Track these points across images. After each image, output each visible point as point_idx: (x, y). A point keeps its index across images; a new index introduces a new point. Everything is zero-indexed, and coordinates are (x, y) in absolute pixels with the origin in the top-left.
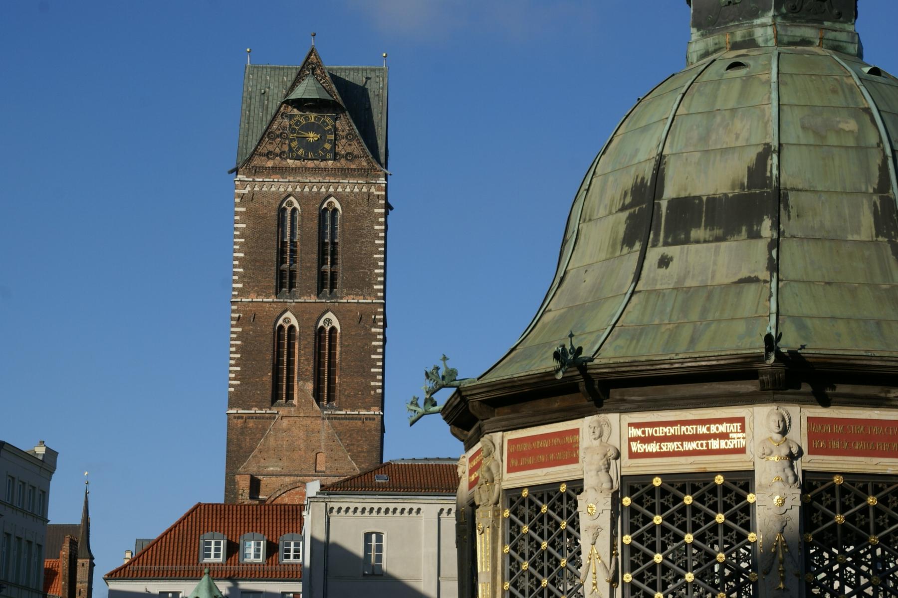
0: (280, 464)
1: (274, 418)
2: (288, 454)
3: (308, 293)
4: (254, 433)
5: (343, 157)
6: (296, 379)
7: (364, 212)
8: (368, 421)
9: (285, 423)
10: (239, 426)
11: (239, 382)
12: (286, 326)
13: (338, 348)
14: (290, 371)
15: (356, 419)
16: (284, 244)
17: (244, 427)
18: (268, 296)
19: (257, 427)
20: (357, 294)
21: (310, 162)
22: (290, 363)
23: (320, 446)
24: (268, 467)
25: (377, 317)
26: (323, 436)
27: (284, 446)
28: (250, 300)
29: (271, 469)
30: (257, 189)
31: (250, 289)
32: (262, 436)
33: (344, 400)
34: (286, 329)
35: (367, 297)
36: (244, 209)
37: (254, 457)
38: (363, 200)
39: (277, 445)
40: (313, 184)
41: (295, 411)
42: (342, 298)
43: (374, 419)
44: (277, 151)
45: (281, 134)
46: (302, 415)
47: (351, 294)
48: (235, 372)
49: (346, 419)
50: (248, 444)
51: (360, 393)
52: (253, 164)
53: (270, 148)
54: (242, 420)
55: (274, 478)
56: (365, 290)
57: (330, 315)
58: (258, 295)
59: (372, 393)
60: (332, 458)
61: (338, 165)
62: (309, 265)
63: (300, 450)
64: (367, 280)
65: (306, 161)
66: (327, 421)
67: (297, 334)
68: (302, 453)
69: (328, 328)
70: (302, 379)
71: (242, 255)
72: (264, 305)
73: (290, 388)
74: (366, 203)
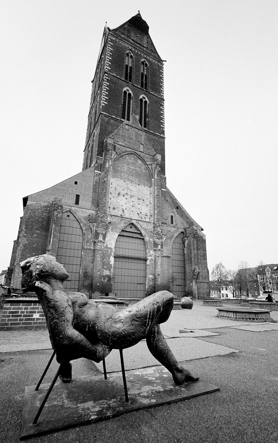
0: (125, 143)
6: (131, 113)
8: (160, 139)
9: (127, 127)
11: (107, 103)
12: (128, 92)
13: (147, 109)
14: (129, 110)
15: (156, 136)
17: (108, 122)
19: (114, 124)
22: (129, 107)
24: (119, 142)
26: (143, 137)
29: (120, 143)
32: (117, 129)
39: (123, 135)
41: (131, 124)
44: (126, 34)
46: (134, 126)
49: (152, 135)
50: (110, 129)
54: (108, 119)
58: (117, 75)
59: (162, 129)
66: (144, 133)
67: (132, 97)
68: (134, 141)
69: (144, 100)
72: (119, 80)
73: (128, 116)
74: (157, 67)
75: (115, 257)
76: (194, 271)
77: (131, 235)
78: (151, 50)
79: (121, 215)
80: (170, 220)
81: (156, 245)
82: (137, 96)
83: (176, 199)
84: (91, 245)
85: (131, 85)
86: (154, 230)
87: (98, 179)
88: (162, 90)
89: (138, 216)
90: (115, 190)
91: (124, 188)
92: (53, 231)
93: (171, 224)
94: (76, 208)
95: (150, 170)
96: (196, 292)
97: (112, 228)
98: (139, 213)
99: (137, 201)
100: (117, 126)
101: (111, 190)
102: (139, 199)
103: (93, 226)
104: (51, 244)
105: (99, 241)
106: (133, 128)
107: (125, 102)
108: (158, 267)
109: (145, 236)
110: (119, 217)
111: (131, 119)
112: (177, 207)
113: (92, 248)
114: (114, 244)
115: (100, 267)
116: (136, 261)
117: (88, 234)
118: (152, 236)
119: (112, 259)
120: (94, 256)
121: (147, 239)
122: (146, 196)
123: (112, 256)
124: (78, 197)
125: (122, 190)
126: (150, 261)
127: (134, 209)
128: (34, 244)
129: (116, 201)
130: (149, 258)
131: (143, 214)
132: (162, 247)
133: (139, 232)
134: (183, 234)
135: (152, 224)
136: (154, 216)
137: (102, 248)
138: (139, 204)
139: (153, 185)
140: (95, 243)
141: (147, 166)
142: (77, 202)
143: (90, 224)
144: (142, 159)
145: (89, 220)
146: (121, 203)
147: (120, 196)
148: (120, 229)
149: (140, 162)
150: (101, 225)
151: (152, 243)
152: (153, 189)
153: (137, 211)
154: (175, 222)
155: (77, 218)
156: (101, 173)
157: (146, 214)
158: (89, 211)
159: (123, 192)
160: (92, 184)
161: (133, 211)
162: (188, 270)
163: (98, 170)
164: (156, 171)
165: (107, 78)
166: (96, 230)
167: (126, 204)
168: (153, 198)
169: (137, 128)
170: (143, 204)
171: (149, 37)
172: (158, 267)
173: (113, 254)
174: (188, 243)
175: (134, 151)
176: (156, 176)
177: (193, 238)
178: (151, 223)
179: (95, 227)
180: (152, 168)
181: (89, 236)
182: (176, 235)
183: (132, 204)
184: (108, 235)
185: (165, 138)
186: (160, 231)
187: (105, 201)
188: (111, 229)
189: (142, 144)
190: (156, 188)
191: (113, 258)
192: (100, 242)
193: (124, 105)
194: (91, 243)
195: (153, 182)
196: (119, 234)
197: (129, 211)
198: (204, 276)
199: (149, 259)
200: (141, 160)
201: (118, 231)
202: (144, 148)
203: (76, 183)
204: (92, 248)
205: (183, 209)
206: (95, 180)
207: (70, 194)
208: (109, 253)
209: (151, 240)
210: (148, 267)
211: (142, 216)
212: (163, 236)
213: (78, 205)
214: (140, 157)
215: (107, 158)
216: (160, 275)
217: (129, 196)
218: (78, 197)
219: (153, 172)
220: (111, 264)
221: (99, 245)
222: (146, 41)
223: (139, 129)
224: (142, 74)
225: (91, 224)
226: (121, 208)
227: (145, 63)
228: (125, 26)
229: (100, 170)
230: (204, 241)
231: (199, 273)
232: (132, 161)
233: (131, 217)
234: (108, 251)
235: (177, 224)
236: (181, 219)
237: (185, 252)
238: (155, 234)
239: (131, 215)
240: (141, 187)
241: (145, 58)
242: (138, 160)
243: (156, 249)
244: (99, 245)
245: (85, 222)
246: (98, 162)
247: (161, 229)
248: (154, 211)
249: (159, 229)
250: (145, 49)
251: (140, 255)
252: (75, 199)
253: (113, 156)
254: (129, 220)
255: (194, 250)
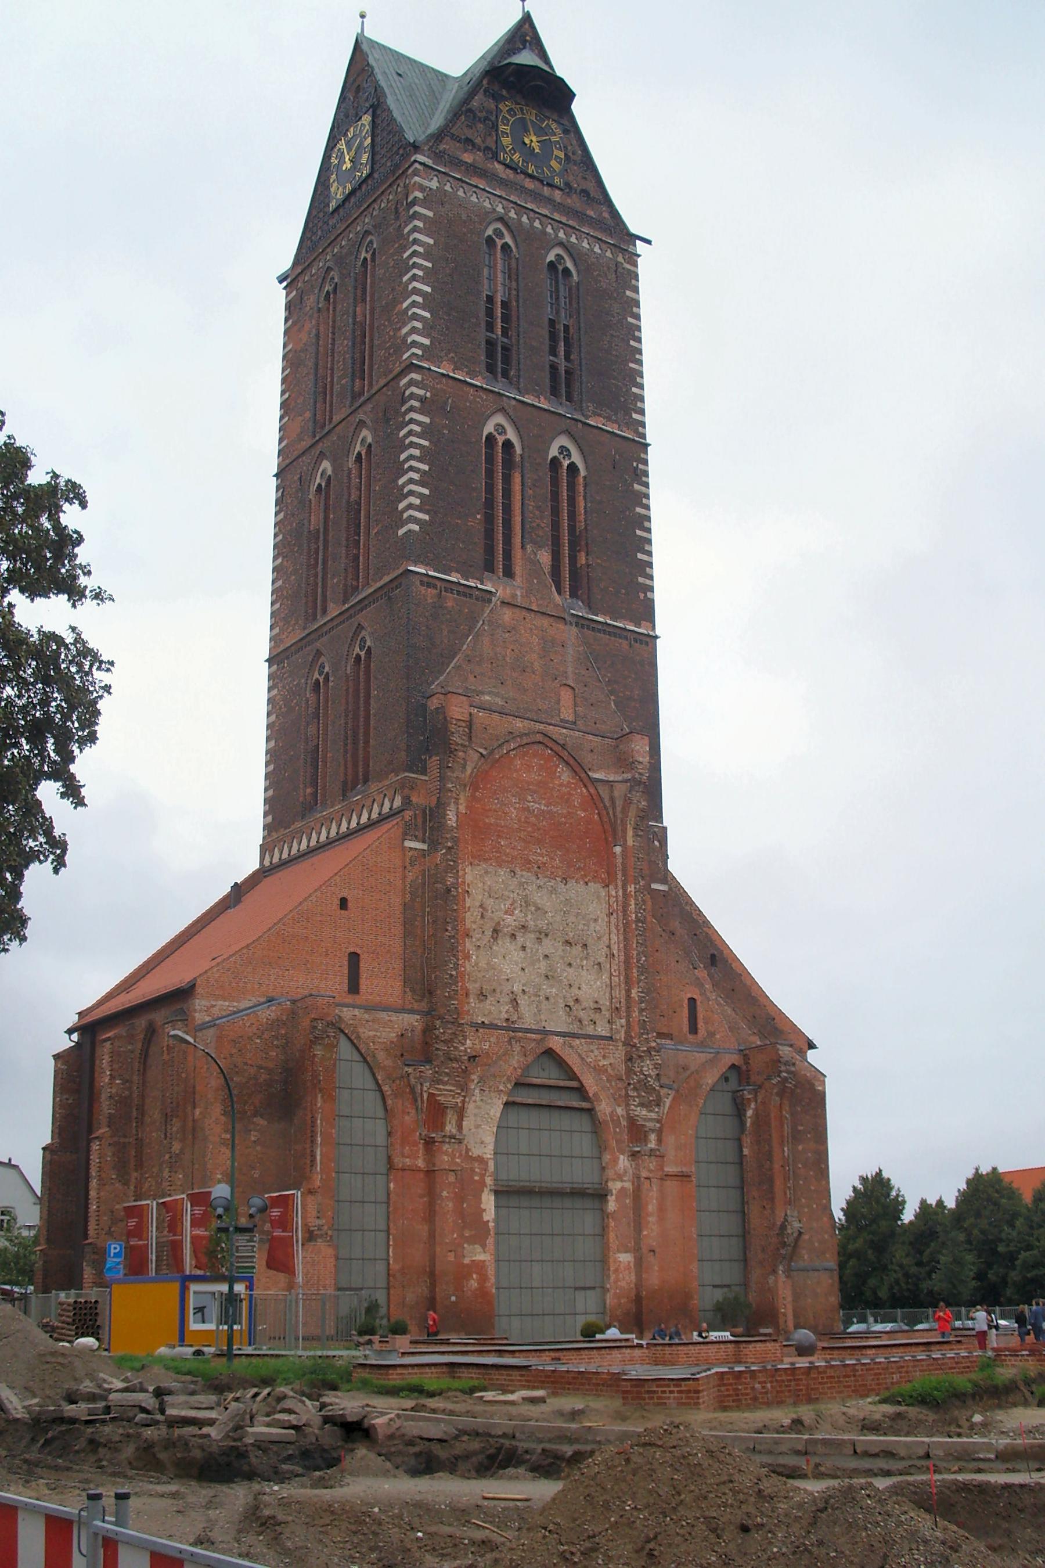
1: (490, 601)
2: (515, 675)
3: (536, 391)
4: (455, 621)
5: (575, 193)
6: (517, 540)
7: (612, 289)
8: (638, 645)
9: (507, 615)
10: (430, 601)
12: (500, 440)
16: (490, 299)
18: (472, 374)
20: (609, 419)
21: (528, 180)
22: (507, 509)
23: (566, 672)
24: (483, 693)
25: (641, 466)
27: (508, 659)
28: (445, 372)
29: (487, 698)
30: (448, 188)
31: (443, 354)
33: (599, 597)
34: (500, 444)
35: (624, 429)
36: (430, 214)
37: (458, 668)
38: (609, 268)
39: (496, 654)
40: (537, 215)
42: (587, 417)
43: (647, 644)
44: (478, 141)
45: (486, 118)
46: (534, 608)
47: (600, 415)
48: (420, 495)
51: (623, 591)
52: (442, 147)
53: (469, 133)
54: (434, 592)
55: (495, 716)
56: (620, 415)
57: (563, 441)
59: (642, 596)
60: (586, 700)
61: (569, 201)
62: (534, 344)
63: (534, 673)
64: (623, 399)
65: (523, 176)
66: (574, 630)
67: (518, 459)
70: (534, 542)
71: (429, 289)
72: (467, 389)
73: (508, 555)
74: (614, 276)
75: (497, 1193)
76: (783, 1227)
77: (545, 1098)
78: (585, 192)
79: (508, 1020)
80: (686, 1021)
81: (636, 1131)
82: (537, 443)
83: (707, 923)
84: (417, 1151)
85: (514, 402)
86: (629, 1071)
87: (417, 877)
88: (635, 395)
89: (570, 1016)
90: (482, 916)
91: (514, 902)
92: (319, 1122)
93: (690, 1037)
94: (357, 1012)
95: (605, 806)
96: (790, 1307)
97: (481, 1079)
98: (571, 1004)
99: (560, 952)
100: (473, 619)
101: (471, 918)
102: (568, 943)
103: (421, 1080)
104: (318, 1169)
105: (444, 1136)
106: (530, 616)
107: (490, 488)
108: (650, 1219)
109: (599, 1100)
110: (501, 1028)
111: (518, 569)
112: (713, 956)
113: (420, 1163)
114: (490, 1140)
115: (455, 1236)
116: (568, 1203)
117: (403, 1112)
118: (623, 1092)
119: (488, 1202)
120: (431, 1193)
121: (604, 1108)
122: (592, 928)
123: (486, 1191)
124: (354, 958)
125: (506, 913)
126: (617, 1200)
127: (554, 990)
128: (254, 1168)
129: (488, 964)
130: (615, 1186)
131: (585, 1004)
132: (660, 1141)
133: (574, 1084)
134: (739, 1072)
135: (620, 1044)
136: (628, 1016)
137: (457, 1164)
138: (570, 965)
139: (619, 876)
140: (429, 1143)
141: (592, 791)
142: (354, 987)
143: (406, 1069)
144: (572, 762)
145: (402, 1055)
146: (508, 969)
147: (500, 942)
148: (509, 1080)
149: (565, 775)
150: (447, 1074)
151: (624, 1123)
152: (620, 893)
153: (565, 997)
154: (706, 1023)
155: (363, 1051)
156: (425, 847)
157: (597, 1002)
158: (401, 1016)
159: (509, 919)
160: (397, 901)
161: (547, 999)
162: (756, 1220)
163: (416, 838)
164: (632, 813)
165: (421, 392)
166: (431, 1095)
167: (523, 969)
168: (621, 931)
169: (543, 613)
170: (585, 962)
171: (572, 129)
172: (650, 1219)
173: (489, 1181)
174: (757, 1114)
175: (542, 727)
176: (630, 833)
177: (777, 1094)
178: (617, 1041)
179: (428, 1084)
180: (612, 799)
181: (407, 1118)
182: (710, 1082)
183: (543, 965)
184: (471, 1108)
185: (656, 637)
186: (653, 1073)
187: (454, 973)
188: (475, 1082)
189: (569, 686)
190: (631, 888)
191: (493, 1198)
192: (447, 1140)
193: (490, 504)
194: (415, 1144)
195: (619, 860)
196: (505, 1100)
197: (533, 998)
198: (816, 1244)
199: (614, 1192)
200: (567, 763)
201: (501, 1087)
202: (575, 705)
203: (344, 903)
204: (420, 1163)
205: (733, 966)
206: (409, 880)
207: (327, 951)
208: (476, 1178)
209: (620, 1111)
210: (612, 1224)
211: (582, 1014)
212: (663, 1091)
213: (357, 997)
214: (565, 754)
215: (450, 786)
216: (657, 1250)
217: (533, 936)
218: (354, 958)
219: (619, 815)
220: (485, 1220)
221: (446, 1153)
222: (562, 155)
223: (553, 616)
224: (552, 323)
225: (410, 1070)
226: (507, 988)
227: (560, 268)
228: (475, 103)
229: (424, 834)
230: (819, 1100)
231: (800, 1233)
232: (534, 777)
233: (544, 1024)
234: (472, 1170)
235: (711, 1034)
236: (729, 1011)
237: (746, 1151)
238: (635, 1089)
239: (542, 1017)
240: (575, 890)
241: (561, 244)
242: (558, 766)
243: (639, 1152)
244: (446, 1153)
245: (389, 1063)
246: (414, 799)
247: (657, 1066)
248: (628, 992)
249: (647, 1067)
250: (557, 195)
251: (581, 1174)
252: (345, 970)
253: (469, 771)
254: (538, 1037)
255: (782, 1144)
